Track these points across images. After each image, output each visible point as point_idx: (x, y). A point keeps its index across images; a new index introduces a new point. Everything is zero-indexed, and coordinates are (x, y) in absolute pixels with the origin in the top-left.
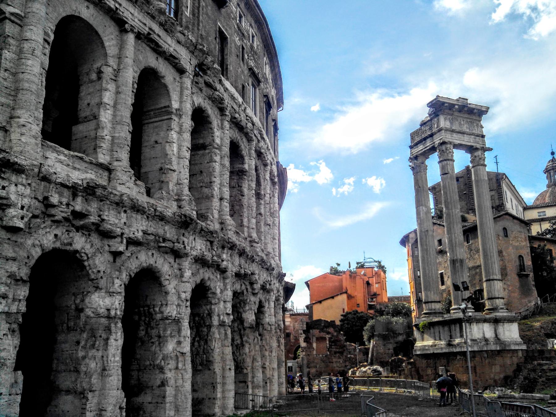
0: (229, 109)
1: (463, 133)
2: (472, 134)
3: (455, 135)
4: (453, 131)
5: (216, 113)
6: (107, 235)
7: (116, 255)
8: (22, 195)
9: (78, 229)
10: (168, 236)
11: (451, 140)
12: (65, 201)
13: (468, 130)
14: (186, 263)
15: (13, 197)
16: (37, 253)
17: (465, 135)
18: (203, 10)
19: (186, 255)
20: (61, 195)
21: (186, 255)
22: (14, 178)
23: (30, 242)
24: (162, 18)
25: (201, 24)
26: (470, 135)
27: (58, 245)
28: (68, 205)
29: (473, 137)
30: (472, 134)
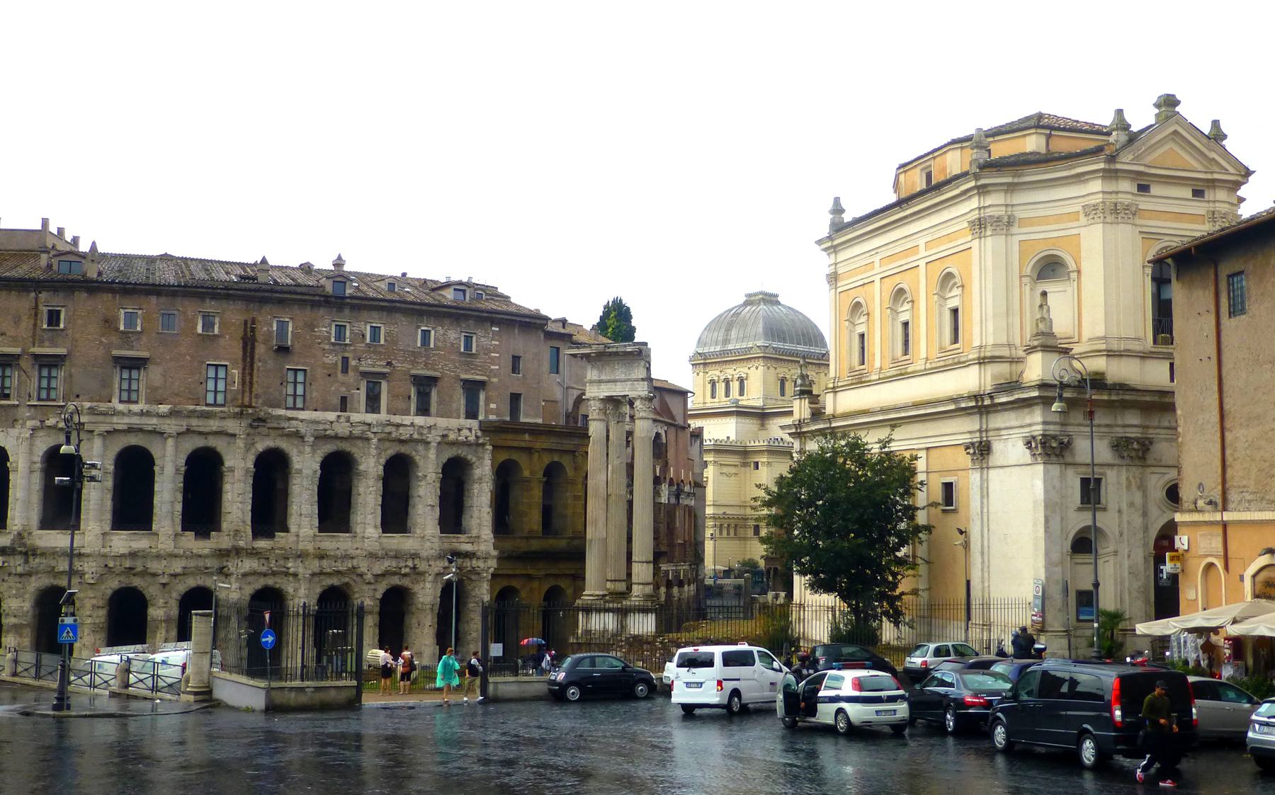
0: (308, 434)
1: (615, 381)
2: (629, 380)
3: (603, 386)
4: (600, 382)
5: (296, 442)
6: (154, 575)
7: (164, 585)
8: (92, 567)
9: (134, 575)
10: (209, 565)
11: (596, 394)
12: (118, 563)
13: (623, 377)
14: (233, 579)
15: (86, 569)
16: (109, 592)
17: (619, 383)
18: (258, 370)
19: (232, 574)
20: (115, 561)
21: (232, 574)
22: (86, 559)
23: (103, 587)
24: (196, 414)
25: (255, 386)
26: (625, 381)
27: (123, 585)
28: (121, 565)
29: (628, 383)
30: (629, 380)
